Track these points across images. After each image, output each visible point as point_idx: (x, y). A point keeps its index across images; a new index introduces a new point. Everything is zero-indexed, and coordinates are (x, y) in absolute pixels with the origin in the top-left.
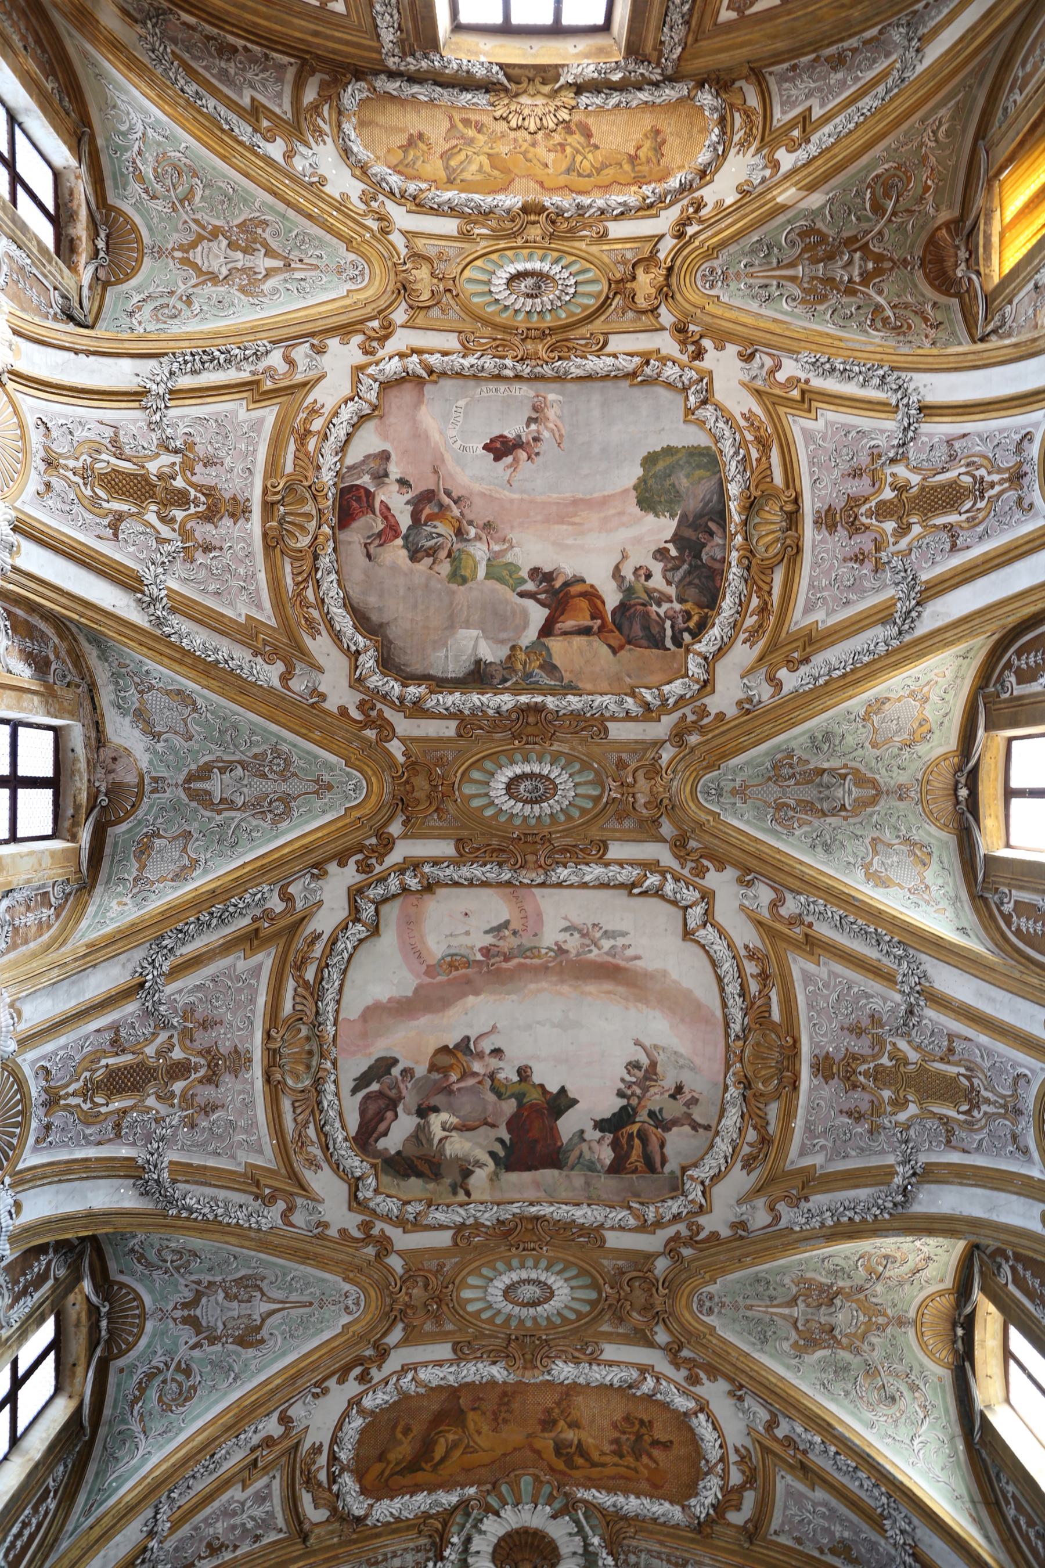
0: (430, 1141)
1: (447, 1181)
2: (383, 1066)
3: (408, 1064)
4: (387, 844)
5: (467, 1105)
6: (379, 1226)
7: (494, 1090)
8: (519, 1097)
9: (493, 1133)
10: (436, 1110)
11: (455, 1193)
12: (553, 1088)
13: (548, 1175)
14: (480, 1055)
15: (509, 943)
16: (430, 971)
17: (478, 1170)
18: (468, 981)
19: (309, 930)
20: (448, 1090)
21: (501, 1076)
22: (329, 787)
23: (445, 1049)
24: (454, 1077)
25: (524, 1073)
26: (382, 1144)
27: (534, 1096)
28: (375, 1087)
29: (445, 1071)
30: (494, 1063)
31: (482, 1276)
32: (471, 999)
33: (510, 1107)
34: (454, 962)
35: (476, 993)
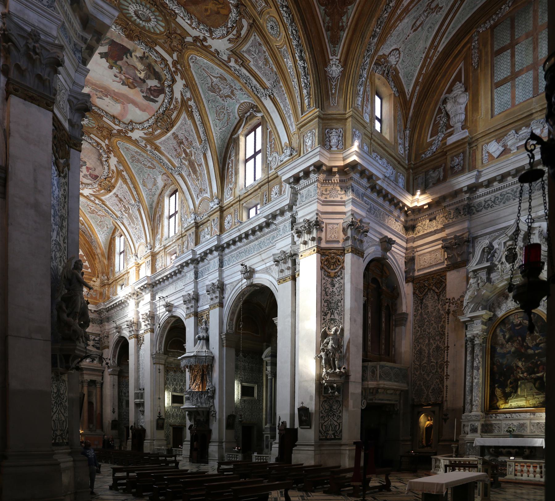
0: (146, 73)
1: (148, 61)
2: (146, 98)
3: (141, 93)
4: (119, 131)
5: (131, 72)
6: (173, 69)
7: (122, 70)
8: (115, 63)
9: (128, 61)
10: (140, 78)
11: (148, 56)
12: (104, 60)
13: (118, 41)
14: (121, 79)
15: (99, 94)
16: (123, 104)
17: (138, 56)
18: (115, 94)
19: (145, 136)
20: (134, 79)
21: (117, 71)
22: (126, 148)
23: (129, 87)
24: (131, 81)
25: (111, 67)
26: (159, 85)
27: (110, 61)
28: (152, 97)
29: (132, 83)
30: (118, 75)
31: (154, 30)
32: (116, 91)
33: (119, 63)
34: (117, 101)
35: (114, 91)
